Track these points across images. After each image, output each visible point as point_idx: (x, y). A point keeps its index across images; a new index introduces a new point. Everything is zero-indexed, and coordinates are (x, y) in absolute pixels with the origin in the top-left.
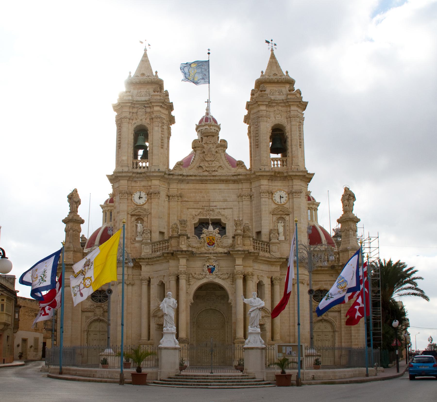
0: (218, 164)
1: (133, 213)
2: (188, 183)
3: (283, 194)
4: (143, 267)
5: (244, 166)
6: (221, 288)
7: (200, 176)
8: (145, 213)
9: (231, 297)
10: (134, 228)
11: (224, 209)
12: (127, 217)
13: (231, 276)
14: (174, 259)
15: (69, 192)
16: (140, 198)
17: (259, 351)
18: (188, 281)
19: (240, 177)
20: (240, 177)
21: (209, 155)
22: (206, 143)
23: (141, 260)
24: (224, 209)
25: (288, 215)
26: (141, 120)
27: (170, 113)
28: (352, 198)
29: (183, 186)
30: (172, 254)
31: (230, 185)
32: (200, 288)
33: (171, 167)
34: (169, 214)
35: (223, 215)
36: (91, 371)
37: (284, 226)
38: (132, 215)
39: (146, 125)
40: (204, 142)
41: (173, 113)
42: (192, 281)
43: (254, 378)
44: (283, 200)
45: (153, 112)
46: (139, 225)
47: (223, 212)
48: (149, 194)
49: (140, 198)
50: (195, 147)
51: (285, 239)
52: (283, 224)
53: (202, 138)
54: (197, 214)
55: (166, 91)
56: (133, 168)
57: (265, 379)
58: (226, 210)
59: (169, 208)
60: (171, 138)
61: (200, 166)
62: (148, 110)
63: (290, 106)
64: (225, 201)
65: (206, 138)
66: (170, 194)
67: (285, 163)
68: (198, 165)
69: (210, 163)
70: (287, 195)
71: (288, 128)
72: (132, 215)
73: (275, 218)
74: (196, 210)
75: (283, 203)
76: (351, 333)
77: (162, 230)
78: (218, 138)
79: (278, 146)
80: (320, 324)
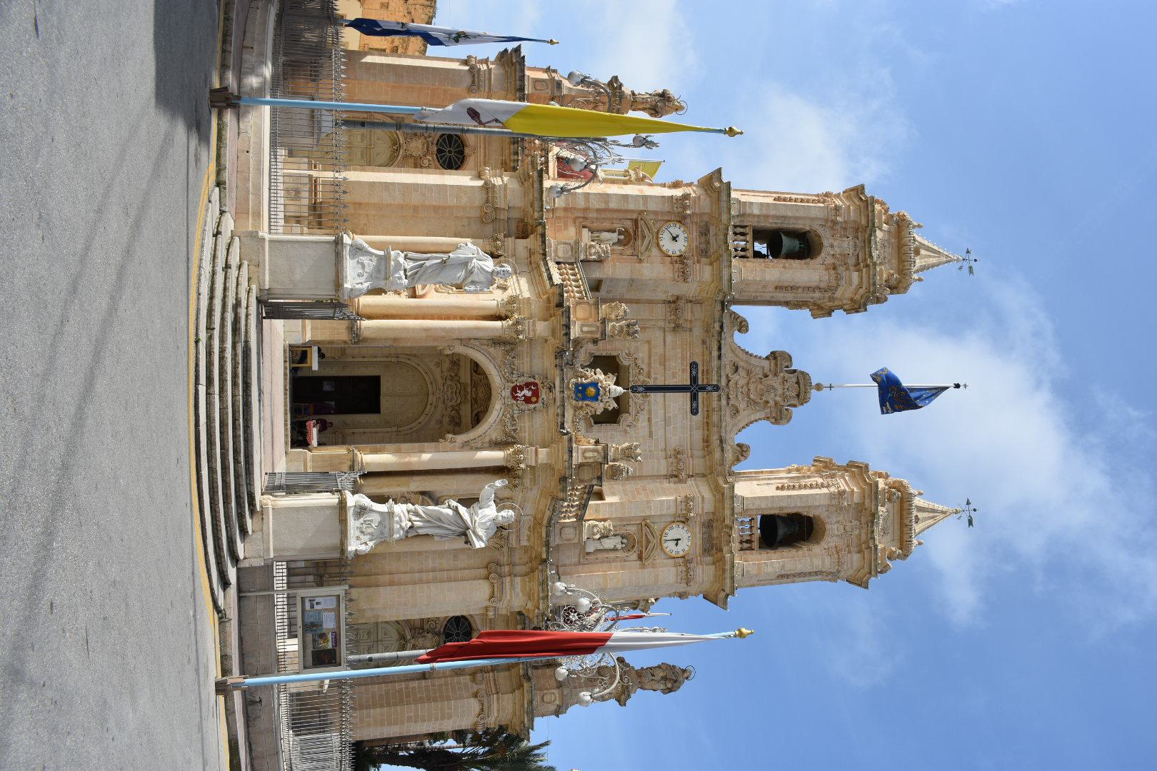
0: (742, 406)
1: (641, 223)
2: (704, 342)
3: (684, 546)
4: (522, 243)
5: (738, 460)
6: (477, 419)
7: (719, 368)
8: (642, 249)
9: (461, 438)
10: (607, 225)
11: (649, 420)
12: (632, 211)
13: (510, 440)
14: (548, 309)
15: (673, 92)
16: (674, 239)
17: (336, 541)
18: (497, 341)
19: (717, 455)
20: (717, 455)
21: (760, 386)
22: (785, 380)
23: (540, 239)
24: (649, 420)
25: (640, 558)
26: (832, 246)
27: (840, 307)
28: (669, 685)
29: (698, 331)
30: (560, 305)
31: (700, 432)
32: (476, 367)
33: (734, 308)
34: (637, 302)
35: (636, 420)
36: (263, 42)
37: (615, 550)
38: (636, 222)
39: (823, 254)
40: (787, 375)
41: (838, 313)
42: (497, 352)
43: (244, 532)
44: (671, 545)
45: (847, 269)
46: (615, 236)
47: (643, 417)
48: (682, 258)
49: (674, 239)
50: (775, 358)
51: (588, 554)
52: (619, 546)
53: (795, 371)
54: (639, 362)
55: (886, 300)
56: (735, 227)
57: (242, 565)
58: (646, 423)
59: (650, 302)
60: (784, 309)
61: (737, 369)
62: (851, 261)
63: (860, 551)
64: (666, 421)
65: (795, 380)
66: (681, 303)
67: (746, 545)
68: (741, 364)
69: (745, 389)
70: (681, 554)
71: (816, 549)
72: (636, 222)
73: (632, 530)
74: (646, 361)
75: (665, 545)
76: (374, 706)
77: (604, 288)
78: (795, 406)
79: (782, 531)
80: (395, 636)
